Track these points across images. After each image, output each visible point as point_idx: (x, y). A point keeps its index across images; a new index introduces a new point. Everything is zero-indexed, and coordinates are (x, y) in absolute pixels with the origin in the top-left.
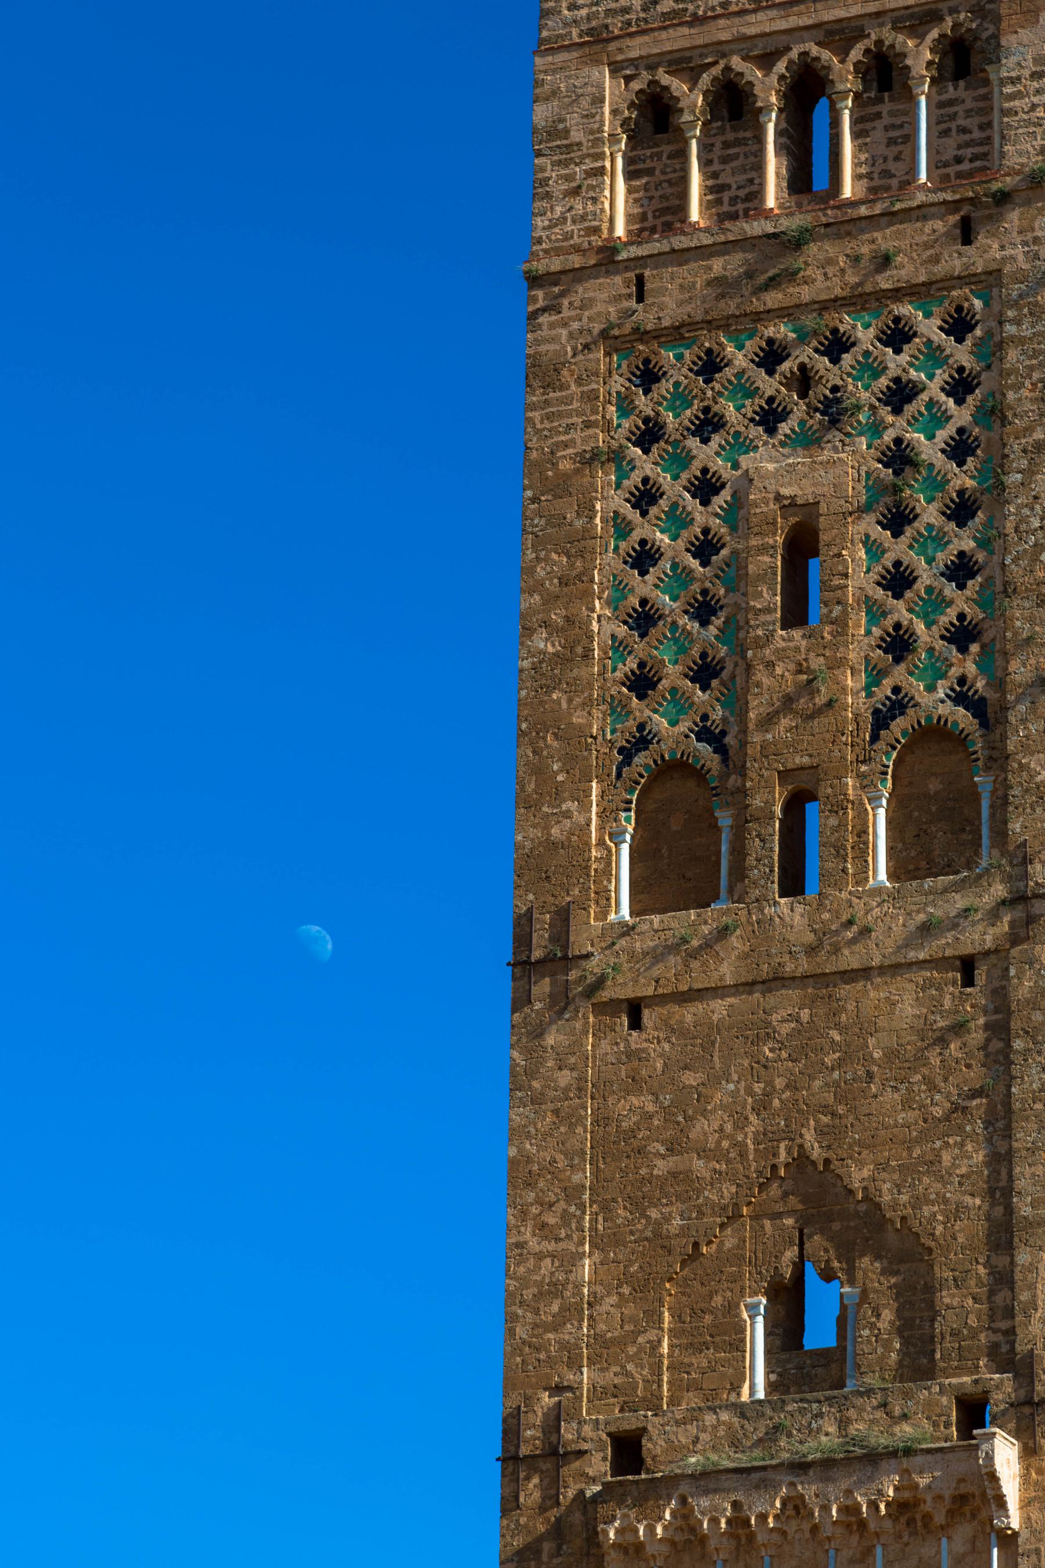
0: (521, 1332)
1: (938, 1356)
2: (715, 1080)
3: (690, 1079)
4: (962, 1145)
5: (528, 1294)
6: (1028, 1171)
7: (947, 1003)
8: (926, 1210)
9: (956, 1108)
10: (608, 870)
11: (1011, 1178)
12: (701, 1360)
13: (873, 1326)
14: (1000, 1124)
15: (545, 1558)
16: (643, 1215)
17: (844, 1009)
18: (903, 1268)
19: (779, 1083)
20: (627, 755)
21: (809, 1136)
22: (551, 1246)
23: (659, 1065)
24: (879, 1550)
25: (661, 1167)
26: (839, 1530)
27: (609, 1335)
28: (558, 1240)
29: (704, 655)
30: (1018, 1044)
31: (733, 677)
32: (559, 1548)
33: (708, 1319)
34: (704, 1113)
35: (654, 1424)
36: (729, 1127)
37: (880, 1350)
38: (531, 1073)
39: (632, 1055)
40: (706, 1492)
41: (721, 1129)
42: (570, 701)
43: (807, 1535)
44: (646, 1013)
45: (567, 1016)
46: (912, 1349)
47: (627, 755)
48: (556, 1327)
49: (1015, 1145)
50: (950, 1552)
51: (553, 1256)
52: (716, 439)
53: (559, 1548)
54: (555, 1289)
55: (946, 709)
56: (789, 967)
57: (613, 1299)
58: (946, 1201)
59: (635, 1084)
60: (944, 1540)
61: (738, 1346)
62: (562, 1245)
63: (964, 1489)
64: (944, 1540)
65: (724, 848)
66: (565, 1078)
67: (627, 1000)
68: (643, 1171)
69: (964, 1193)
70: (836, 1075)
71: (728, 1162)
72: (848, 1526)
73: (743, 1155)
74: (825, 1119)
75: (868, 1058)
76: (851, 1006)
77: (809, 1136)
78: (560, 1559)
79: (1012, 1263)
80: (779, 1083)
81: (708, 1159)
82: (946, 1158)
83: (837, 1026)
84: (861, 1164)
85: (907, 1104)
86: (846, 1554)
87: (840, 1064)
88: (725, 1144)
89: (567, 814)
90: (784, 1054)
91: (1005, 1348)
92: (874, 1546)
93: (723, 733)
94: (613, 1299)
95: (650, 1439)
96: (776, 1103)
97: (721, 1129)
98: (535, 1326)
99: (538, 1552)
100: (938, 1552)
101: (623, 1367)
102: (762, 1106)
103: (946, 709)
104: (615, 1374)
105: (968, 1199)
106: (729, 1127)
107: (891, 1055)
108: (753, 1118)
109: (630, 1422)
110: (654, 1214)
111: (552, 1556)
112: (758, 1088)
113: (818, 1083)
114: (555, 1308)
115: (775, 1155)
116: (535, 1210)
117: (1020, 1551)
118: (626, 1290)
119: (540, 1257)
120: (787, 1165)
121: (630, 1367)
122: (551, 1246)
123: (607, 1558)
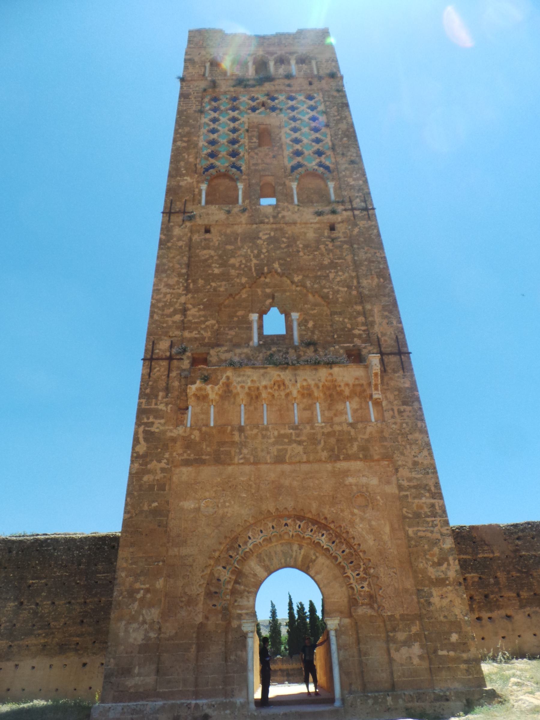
0: (156, 317)
1: (336, 336)
2: (239, 248)
3: (229, 247)
4: (337, 272)
5: (160, 305)
6: (365, 282)
7: (326, 234)
8: (326, 291)
9: (332, 262)
10: (200, 194)
11: (358, 283)
12: (232, 333)
13: (305, 326)
14: (351, 268)
15: (160, 398)
16: (209, 284)
17: (287, 233)
18: (316, 308)
19: (264, 251)
20: (207, 170)
21: (276, 265)
22: (171, 291)
23: (217, 244)
24: (318, 404)
25: (216, 271)
26: (299, 397)
27: (193, 321)
28: (174, 289)
29: (233, 151)
30: (355, 246)
31: (244, 156)
32: (167, 395)
33: (236, 319)
34: (234, 257)
35: (212, 352)
36: (244, 262)
37: (310, 334)
38: (168, 241)
39: (205, 239)
40: (239, 376)
41: (241, 261)
42: (188, 156)
43: (283, 397)
44: (212, 230)
45: (182, 227)
46: (323, 334)
47: (207, 170)
48: (170, 316)
49: (360, 273)
50: (351, 408)
51: (172, 294)
52: (237, 112)
53: (167, 395)
54: (171, 304)
55: (316, 167)
56: (266, 220)
57: (196, 309)
58: (333, 288)
59: (207, 247)
60: (348, 403)
61: (250, 328)
62: (174, 291)
63: (357, 382)
64: (348, 403)
65: (240, 193)
66: (180, 243)
67: (205, 225)
68: (210, 272)
69: (340, 286)
70: (285, 250)
71: (244, 271)
72: (303, 395)
73: (250, 269)
74: (281, 261)
75: (297, 246)
76: (289, 232)
77: (276, 265)
78: (167, 399)
79: (364, 308)
80: (264, 251)
81: (236, 270)
82: (332, 276)
83: (285, 237)
84: (298, 275)
85: (314, 259)
86: (302, 406)
87: (288, 247)
88: (243, 266)
89: (186, 180)
90: (265, 243)
91: (364, 336)
92: (315, 403)
93: (241, 167)
94: (196, 309)
95: (211, 356)
96: (262, 256)
97: (241, 261)
98: (162, 315)
99: (156, 396)
100: (345, 407)
101: (199, 332)
102: (257, 257)
103: (316, 167)
104: (196, 334)
105: (341, 289)
106: (244, 262)
107: (306, 246)
108: (253, 259)
109: (203, 350)
110: (213, 284)
111: (163, 398)
112: (256, 252)
113: (278, 252)
114: (172, 310)
115: (264, 270)
116: (165, 279)
117: (384, 409)
118: (202, 307)
119: (165, 294)
120: (268, 273)
121: (202, 332)
122: (171, 291)
123: (189, 400)
